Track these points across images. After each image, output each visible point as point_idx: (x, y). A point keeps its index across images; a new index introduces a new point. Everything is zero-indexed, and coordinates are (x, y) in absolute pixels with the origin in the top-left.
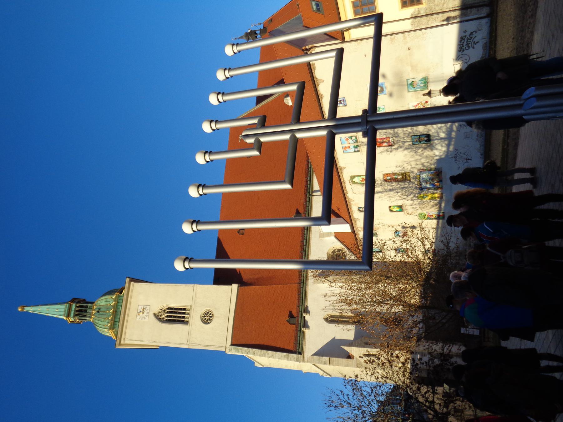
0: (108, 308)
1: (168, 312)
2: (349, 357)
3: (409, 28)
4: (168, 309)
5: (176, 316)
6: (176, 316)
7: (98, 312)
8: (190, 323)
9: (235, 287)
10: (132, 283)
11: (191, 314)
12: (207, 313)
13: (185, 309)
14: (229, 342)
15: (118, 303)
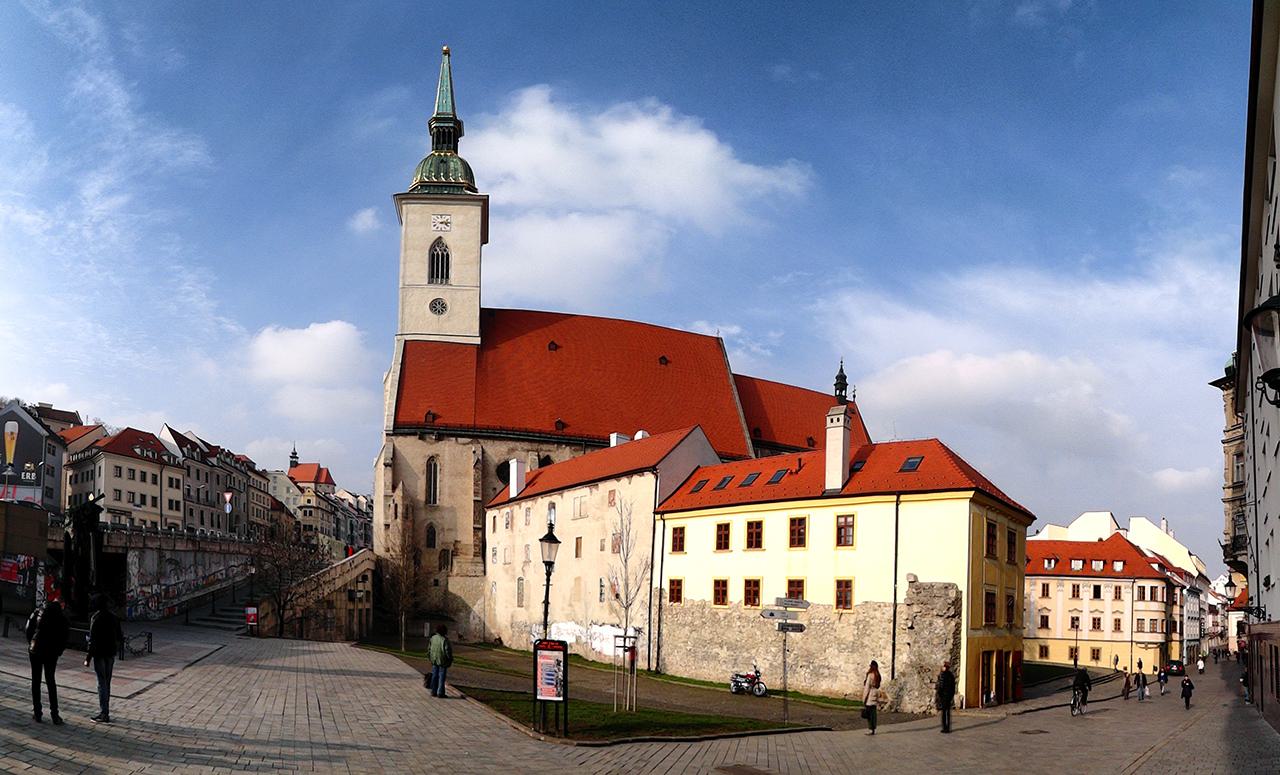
0: (446, 176)
1: (443, 254)
2: (394, 488)
3: (654, 586)
4: (448, 255)
5: (439, 265)
6: (439, 265)
7: (442, 161)
8: (431, 286)
9: (478, 341)
10: (481, 203)
11: (441, 286)
12: (444, 307)
13: (447, 277)
14: (408, 338)
15: (454, 186)
